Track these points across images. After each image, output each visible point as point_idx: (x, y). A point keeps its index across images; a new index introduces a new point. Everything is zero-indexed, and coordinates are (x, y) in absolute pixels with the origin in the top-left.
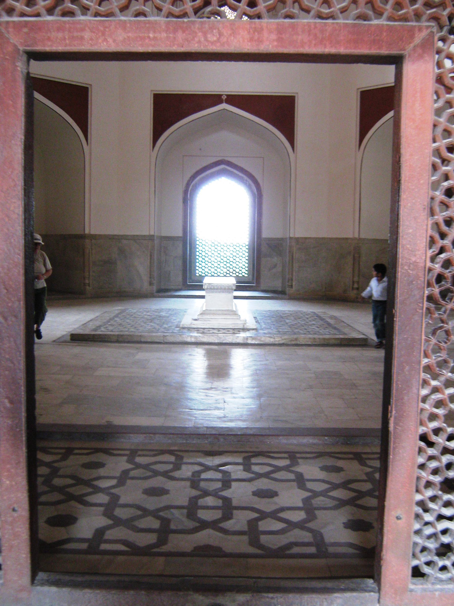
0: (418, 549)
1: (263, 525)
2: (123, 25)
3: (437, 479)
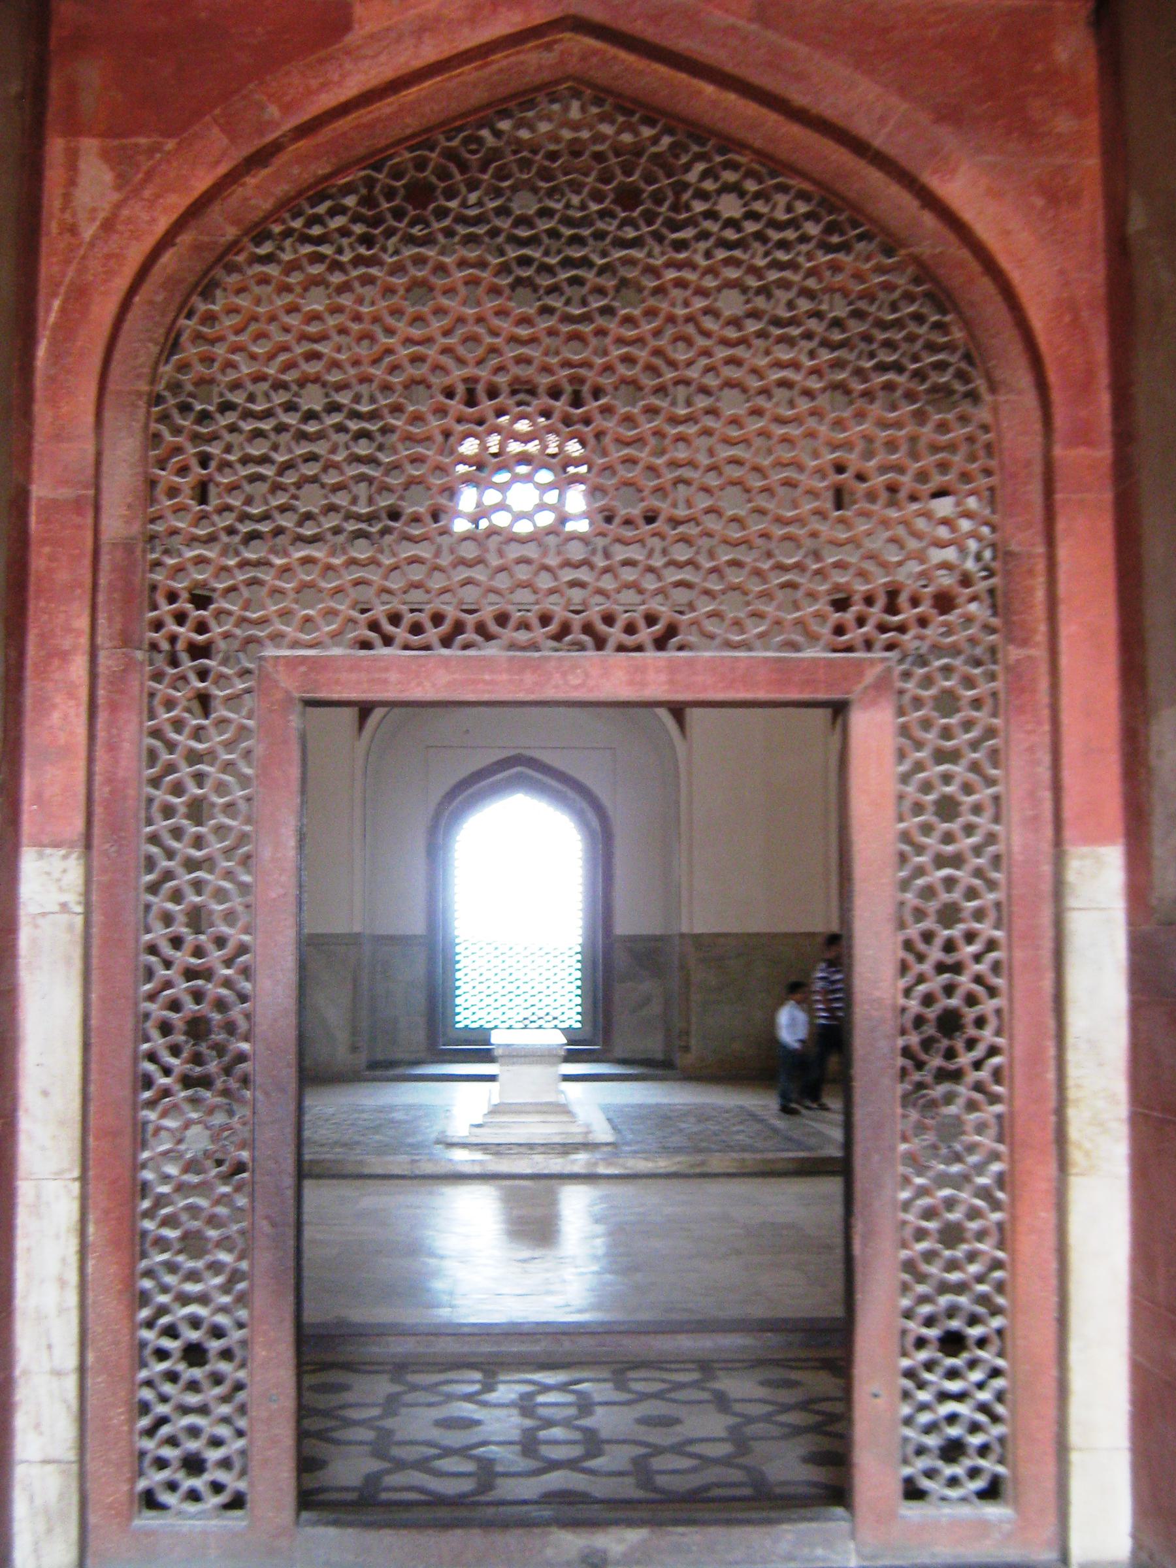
0: (910, 1449)
1: (657, 1463)
2: (445, 662)
3: (932, 1333)
